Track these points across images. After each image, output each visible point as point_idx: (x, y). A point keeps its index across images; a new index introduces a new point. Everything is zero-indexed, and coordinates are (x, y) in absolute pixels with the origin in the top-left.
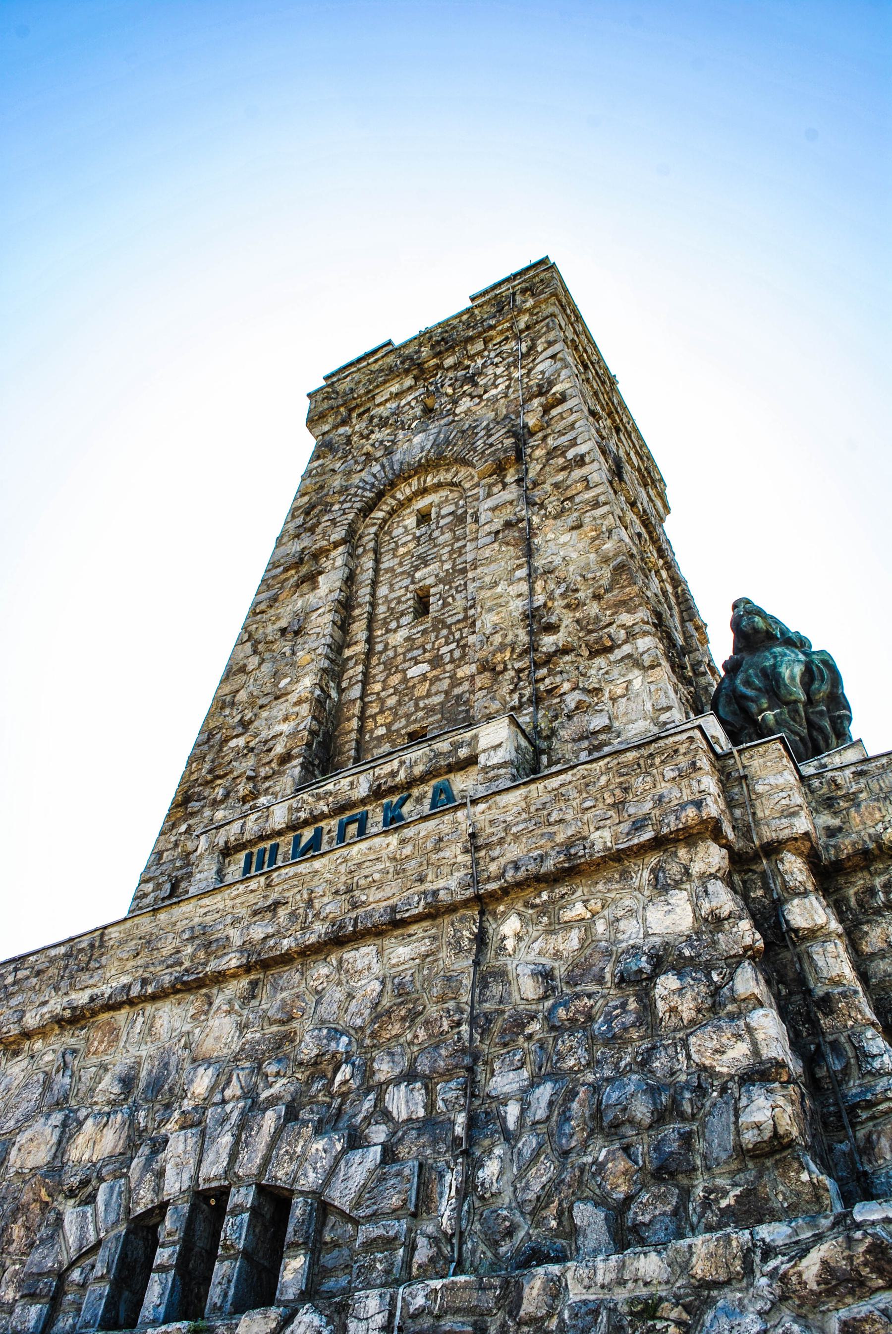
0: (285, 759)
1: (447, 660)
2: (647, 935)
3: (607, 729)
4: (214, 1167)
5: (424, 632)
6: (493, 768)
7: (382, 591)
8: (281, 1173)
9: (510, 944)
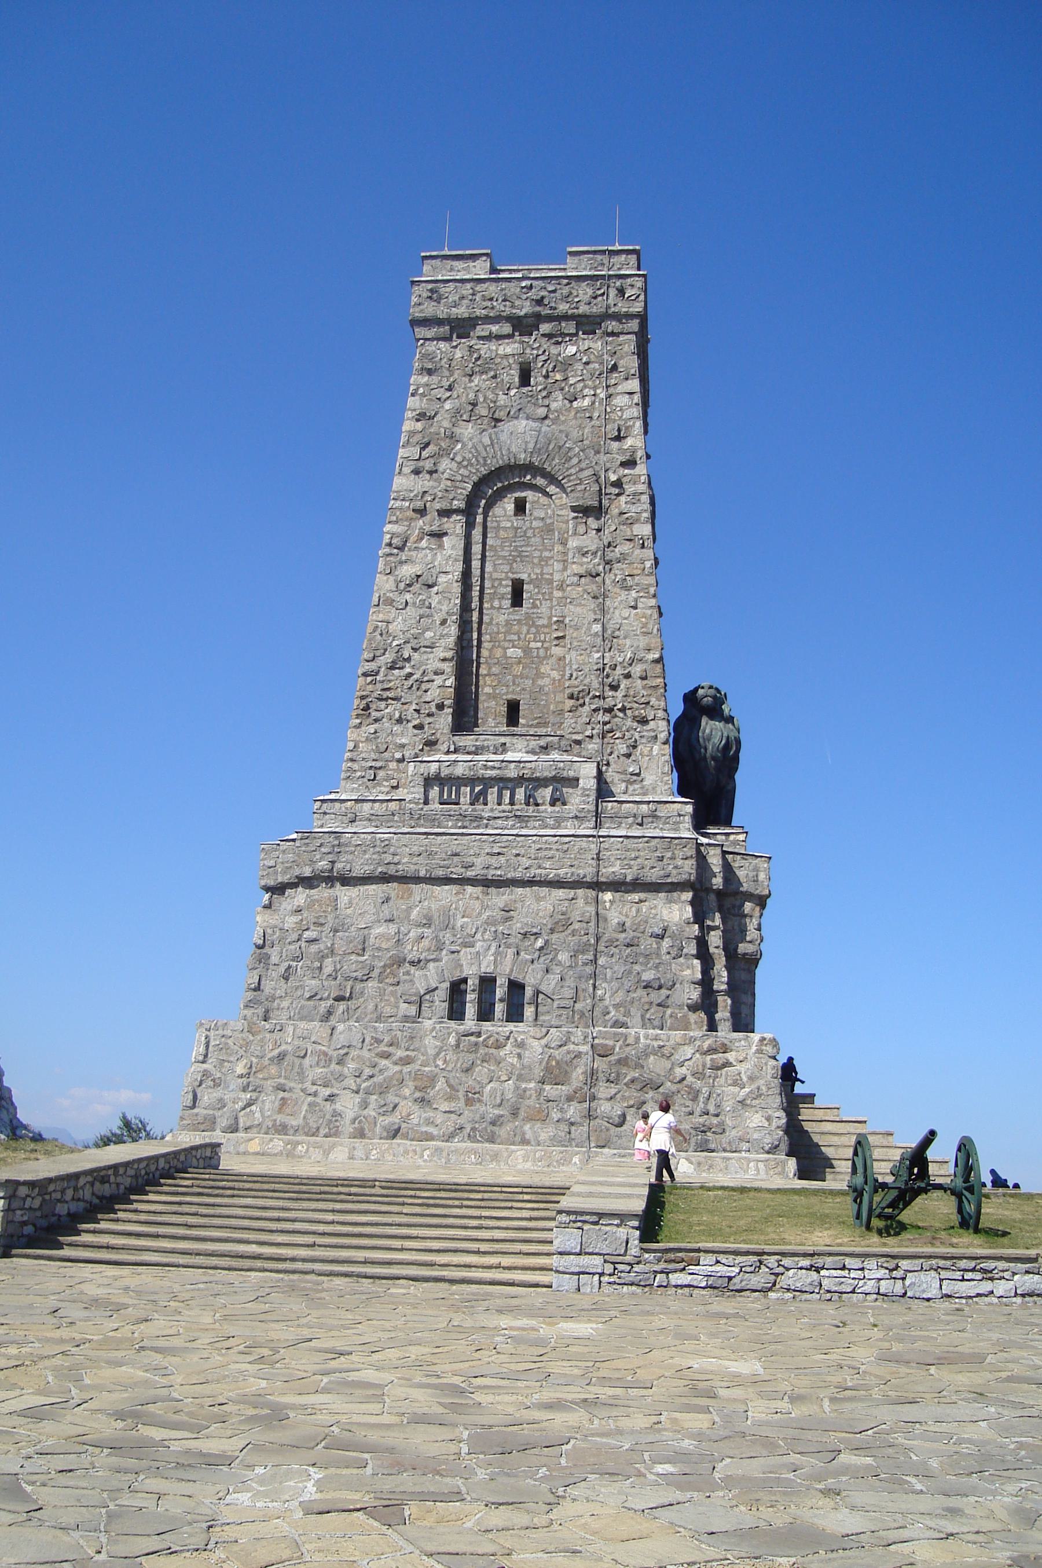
0: (440, 707)
1: (535, 654)
3: (638, 775)
4: (487, 967)
5: (519, 621)
7: (489, 568)
9: (608, 905)
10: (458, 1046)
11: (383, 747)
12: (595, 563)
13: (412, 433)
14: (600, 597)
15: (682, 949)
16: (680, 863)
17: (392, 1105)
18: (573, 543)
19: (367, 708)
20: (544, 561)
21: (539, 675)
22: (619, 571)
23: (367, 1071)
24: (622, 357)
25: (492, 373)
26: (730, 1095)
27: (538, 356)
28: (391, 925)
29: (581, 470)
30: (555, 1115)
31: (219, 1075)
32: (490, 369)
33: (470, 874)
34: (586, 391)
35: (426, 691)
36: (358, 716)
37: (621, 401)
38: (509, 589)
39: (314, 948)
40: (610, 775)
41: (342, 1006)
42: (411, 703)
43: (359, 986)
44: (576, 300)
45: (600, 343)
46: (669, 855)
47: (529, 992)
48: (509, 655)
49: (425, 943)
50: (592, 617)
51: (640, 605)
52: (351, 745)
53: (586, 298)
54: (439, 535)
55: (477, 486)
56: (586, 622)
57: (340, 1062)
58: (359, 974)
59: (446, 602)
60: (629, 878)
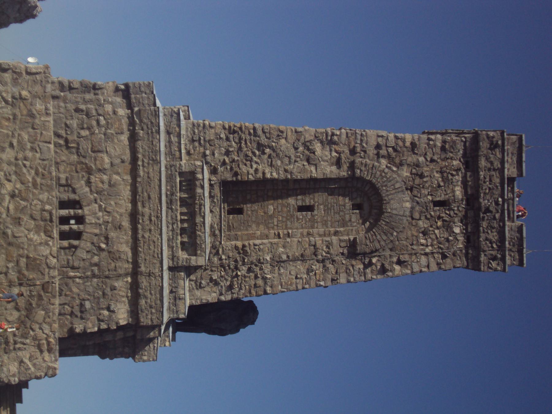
1: (270, 221)
2: (118, 309)
5: (289, 211)
6: (190, 261)
8: (85, 236)
9: (126, 280)
10: (44, 210)
11: (212, 143)
13: (404, 140)
14: (303, 258)
15: (103, 321)
16: (149, 317)
17: (10, 178)
18: (335, 239)
19: (234, 132)
20: (325, 224)
21: (258, 224)
22: (317, 267)
23: (27, 163)
24: (452, 260)
25: (442, 184)
26: (25, 355)
27: (453, 210)
28: (110, 165)
29: (379, 242)
30: (10, 265)
31: (20, 81)
32: (445, 183)
33: (139, 204)
34: (429, 240)
35: (246, 165)
36: (230, 127)
38: (308, 204)
39: (94, 123)
40: (199, 273)
41: (62, 142)
42: (238, 156)
43: (74, 150)
44: (489, 232)
45: (461, 246)
46: (154, 311)
47: (75, 243)
48: (269, 207)
49: (101, 185)
50: (290, 255)
51: (298, 281)
52: (213, 124)
53: (490, 237)
54: (338, 163)
55: (370, 182)
56: (288, 250)
57: (33, 149)
58: (81, 150)
59: (299, 170)
60: (141, 291)
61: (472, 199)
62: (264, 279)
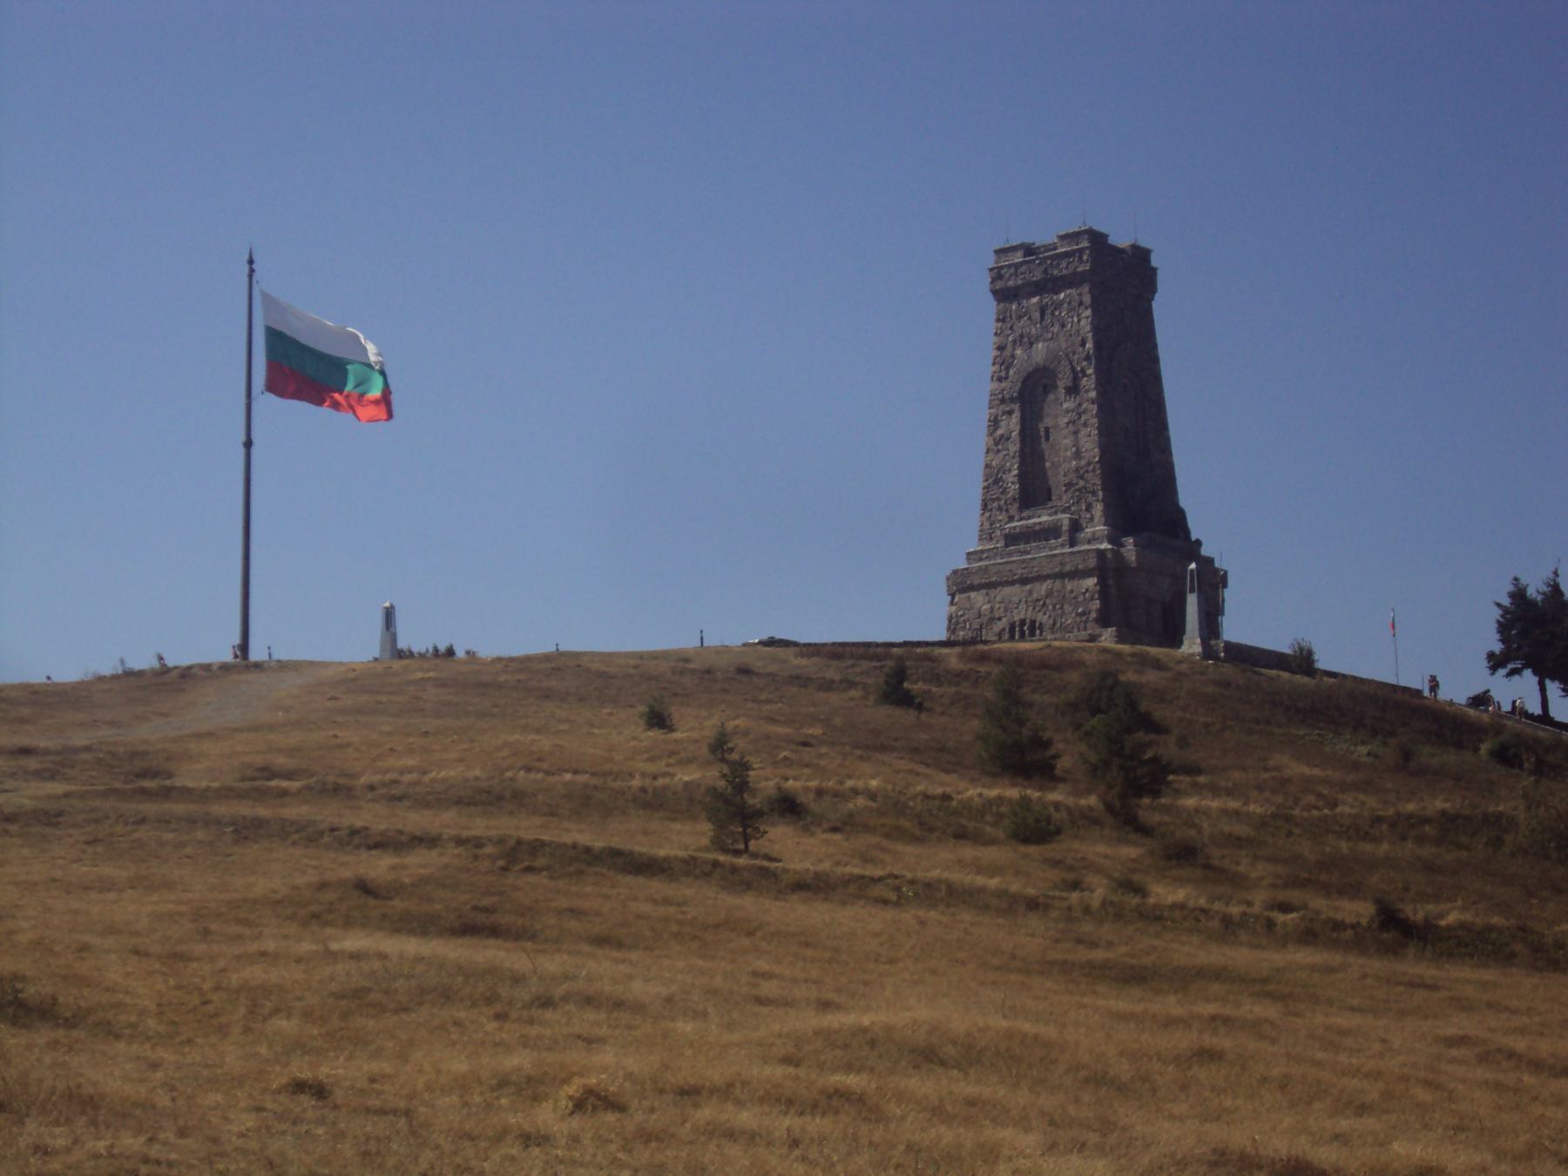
12: (1074, 416)
37: (1083, 322)
54: (1010, 413)
59: (1014, 447)
61: (1039, 288)
62: (1089, 463)
